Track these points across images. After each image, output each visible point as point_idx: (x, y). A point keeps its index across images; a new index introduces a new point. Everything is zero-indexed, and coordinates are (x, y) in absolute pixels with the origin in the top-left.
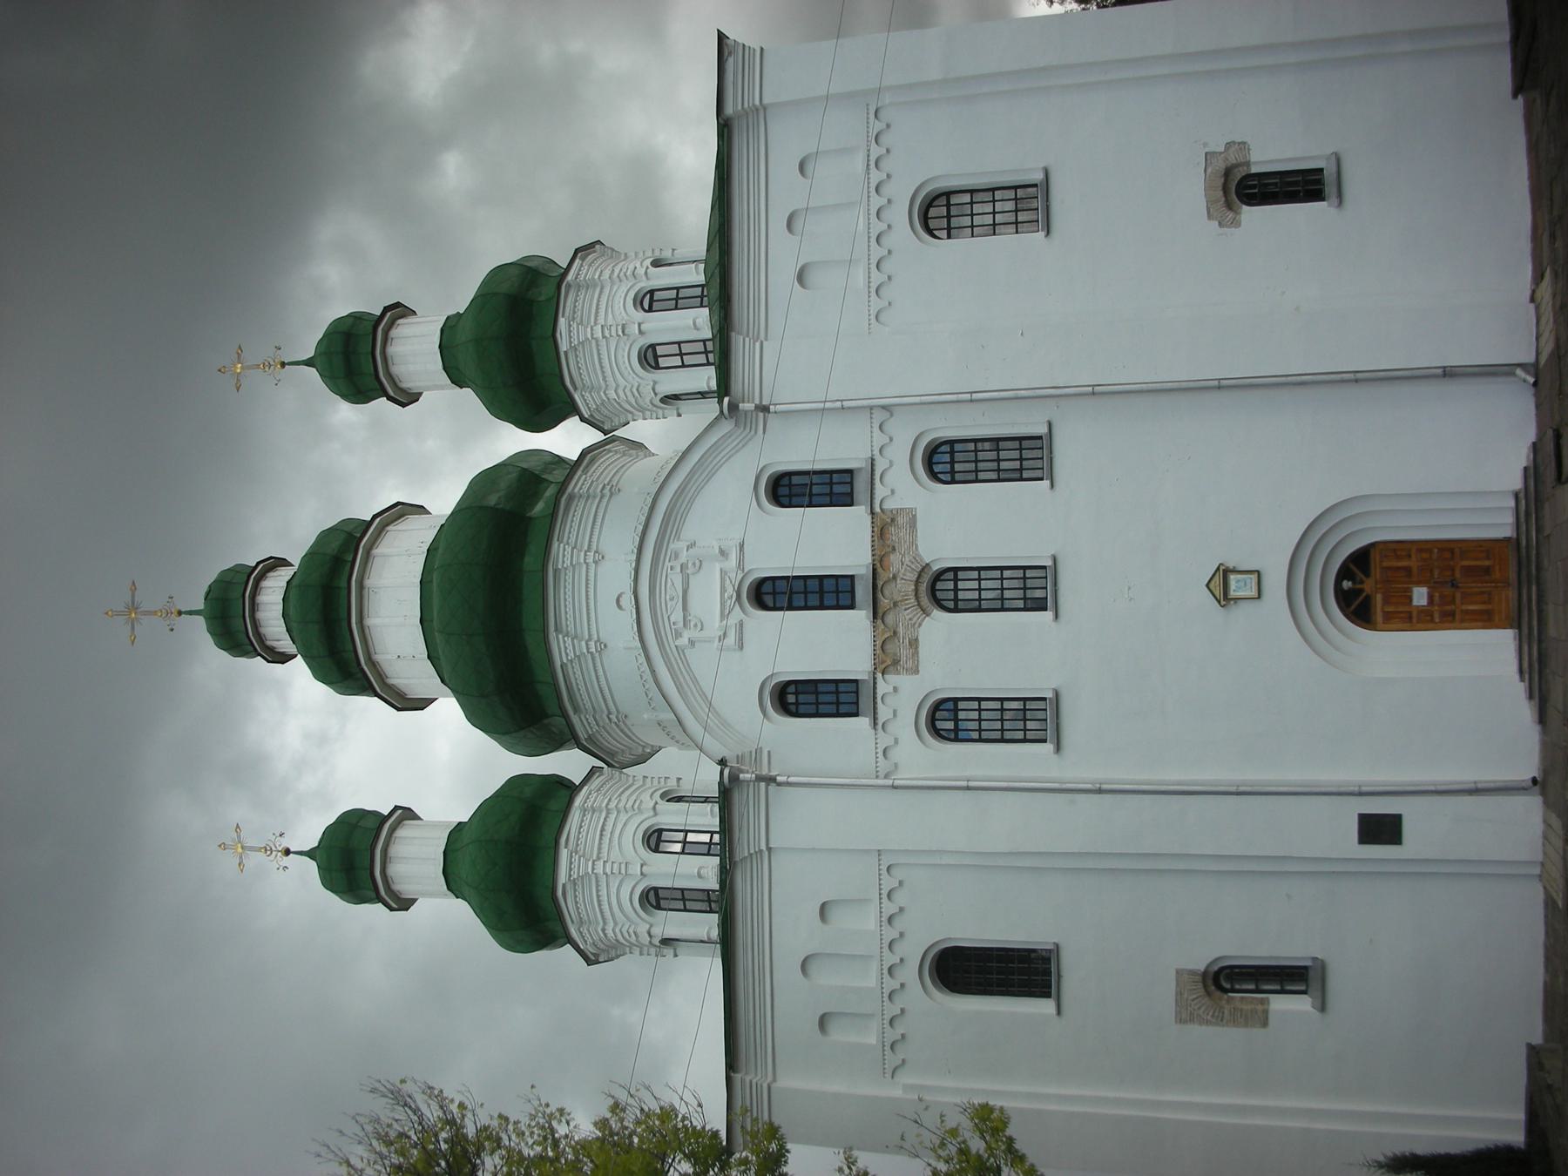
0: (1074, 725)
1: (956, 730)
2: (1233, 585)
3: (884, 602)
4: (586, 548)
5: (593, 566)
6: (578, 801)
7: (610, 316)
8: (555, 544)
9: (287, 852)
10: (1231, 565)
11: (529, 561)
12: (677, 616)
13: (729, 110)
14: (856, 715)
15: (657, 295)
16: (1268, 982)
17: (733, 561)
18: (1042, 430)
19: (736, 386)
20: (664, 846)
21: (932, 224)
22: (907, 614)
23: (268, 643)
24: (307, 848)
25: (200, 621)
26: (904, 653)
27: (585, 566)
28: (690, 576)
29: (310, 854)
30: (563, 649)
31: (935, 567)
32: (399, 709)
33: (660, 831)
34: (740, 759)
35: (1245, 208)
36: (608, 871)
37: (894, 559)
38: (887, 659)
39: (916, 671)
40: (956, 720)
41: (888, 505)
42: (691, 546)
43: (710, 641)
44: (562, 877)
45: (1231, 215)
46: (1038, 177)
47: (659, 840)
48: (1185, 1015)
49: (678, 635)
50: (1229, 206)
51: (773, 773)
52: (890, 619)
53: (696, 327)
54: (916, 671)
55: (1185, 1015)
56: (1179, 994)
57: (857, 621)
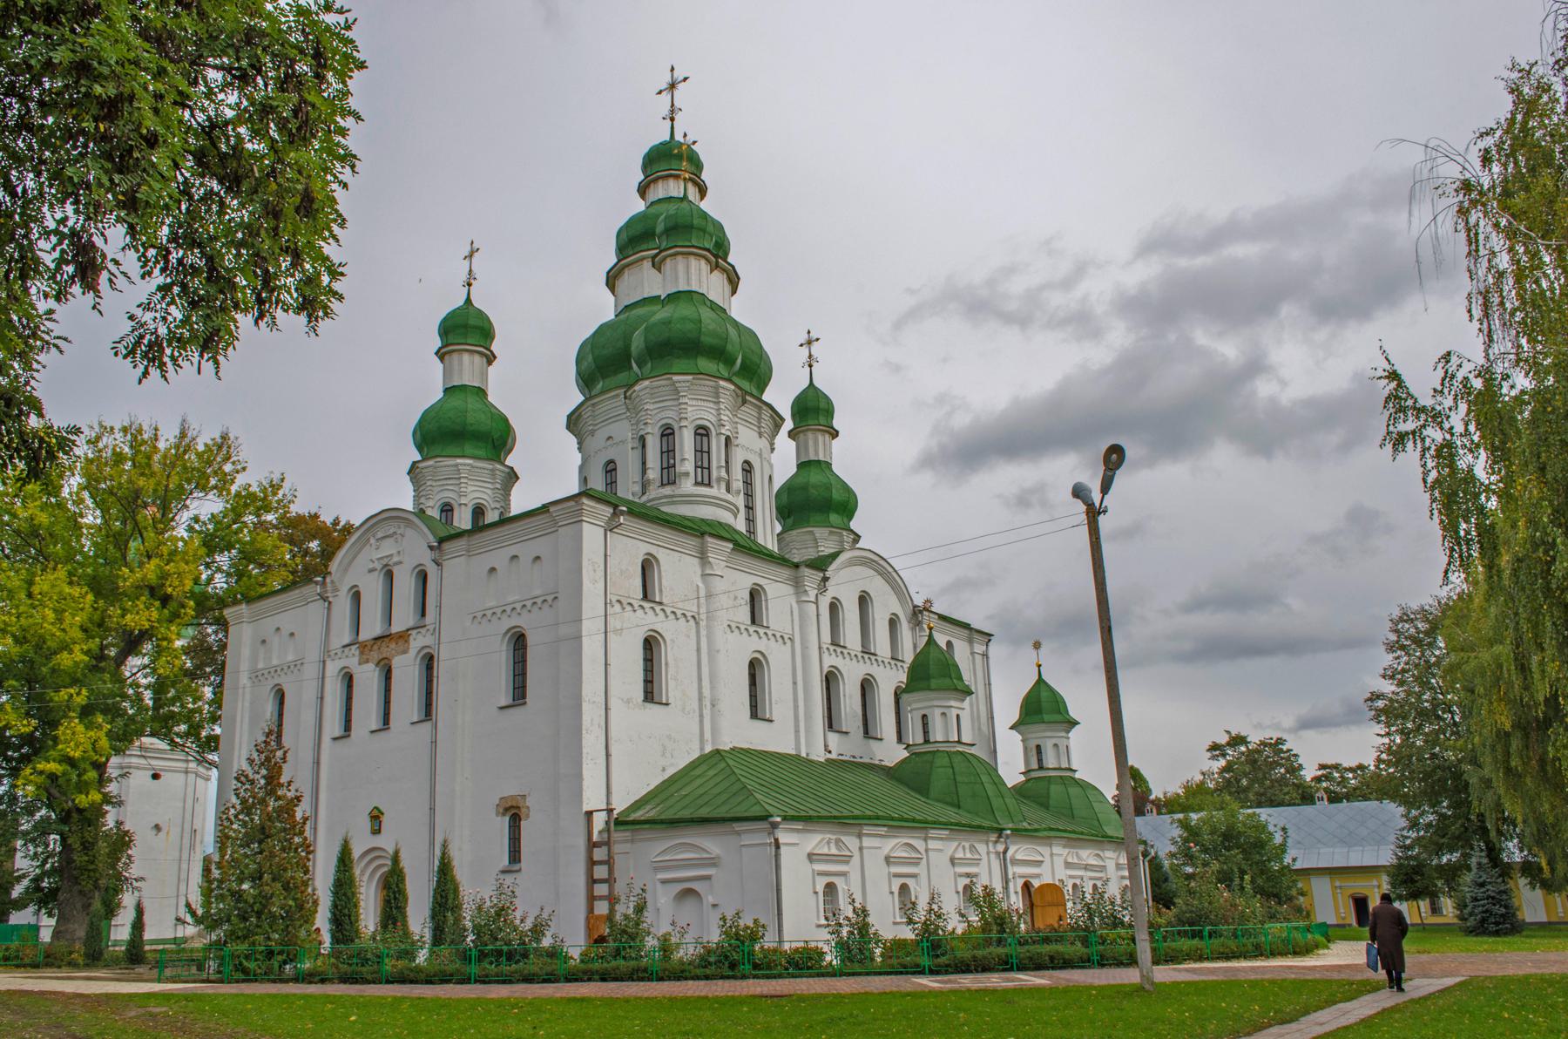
3: (379, 642)
5: (624, 416)
6: (459, 461)
10: (385, 819)
12: (380, 535)
13: (551, 509)
15: (671, 437)
17: (396, 559)
19: (446, 546)
20: (444, 514)
22: (376, 656)
24: (472, 297)
25: (668, 139)
29: (468, 301)
34: (332, 582)
35: (507, 818)
37: (393, 645)
39: (360, 664)
41: (411, 638)
42: (402, 536)
45: (501, 810)
47: (447, 511)
50: (507, 810)
51: (330, 599)
54: (360, 664)
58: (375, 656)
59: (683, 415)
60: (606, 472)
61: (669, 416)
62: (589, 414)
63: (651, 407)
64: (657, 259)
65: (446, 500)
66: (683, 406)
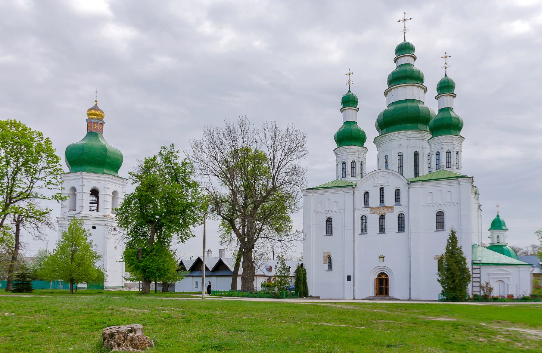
0: (363, 236)
1: (363, 219)
2: (382, 258)
3: (380, 208)
4: (410, 137)
6: (359, 147)
7: (445, 145)
8: (411, 131)
9: (349, 85)
10: (385, 258)
11: (409, 125)
12: (378, 176)
14: (365, 204)
15: (449, 154)
16: (330, 264)
17: (386, 184)
18: (405, 231)
21: (439, 213)
22: (378, 212)
23: (397, 60)
26: (373, 212)
27: (407, 137)
28: (384, 178)
30: (391, 134)
31: (385, 216)
32: (384, 94)
33: (355, 163)
35: (437, 261)
36: (348, 155)
38: (372, 209)
39: (370, 214)
40: (364, 219)
43: (375, 182)
44: (346, 147)
45: (436, 258)
46: (445, 230)
47: (353, 163)
48: (325, 253)
49: (375, 176)
50: (438, 258)
51: (355, 193)
52: (378, 209)
53: (442, 162)
55: (325, 253)
56: (327, 252)
57: (378, 204)
58: (378, 211)
59: (454, 148)
60: (398, 155)
61: (450, 147)
62: (393, 136)
63: (444, 144)
64: (437, 97)
65: (354, 160)
66: (454, 145)
